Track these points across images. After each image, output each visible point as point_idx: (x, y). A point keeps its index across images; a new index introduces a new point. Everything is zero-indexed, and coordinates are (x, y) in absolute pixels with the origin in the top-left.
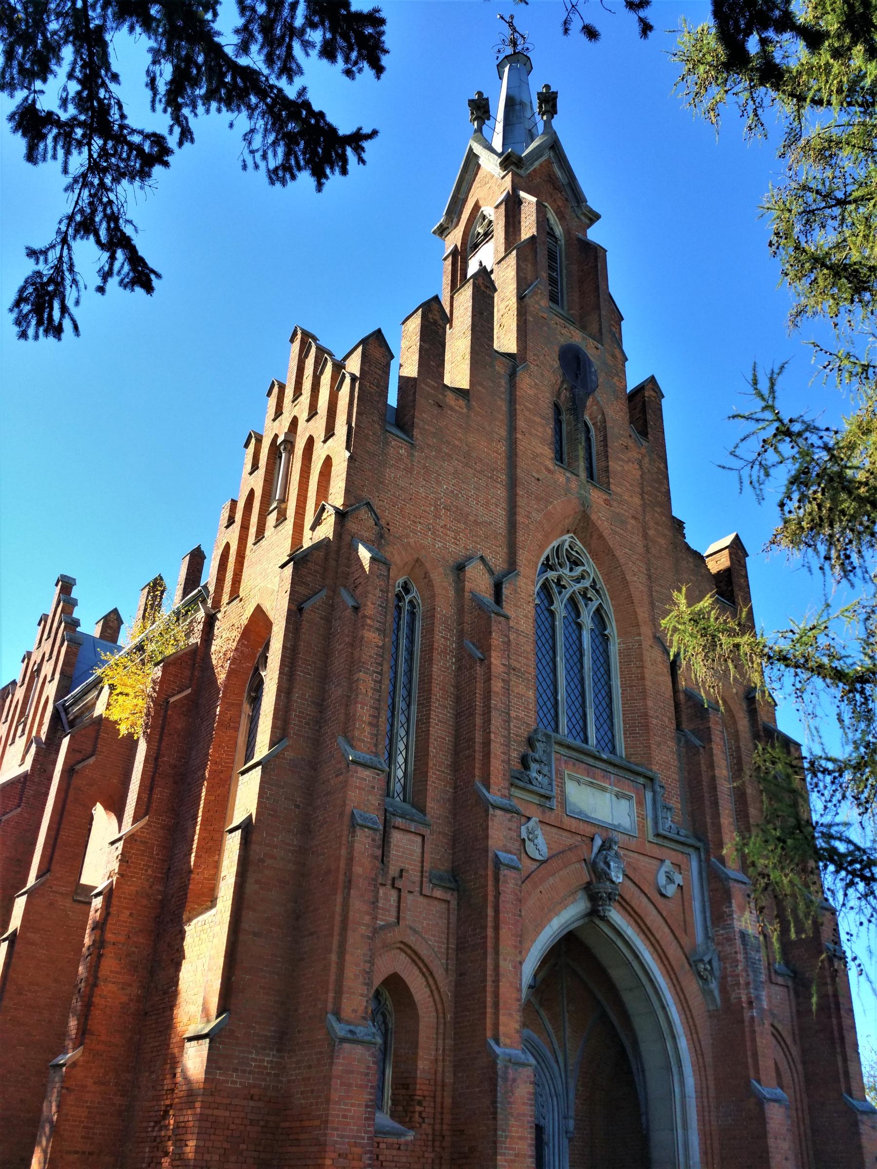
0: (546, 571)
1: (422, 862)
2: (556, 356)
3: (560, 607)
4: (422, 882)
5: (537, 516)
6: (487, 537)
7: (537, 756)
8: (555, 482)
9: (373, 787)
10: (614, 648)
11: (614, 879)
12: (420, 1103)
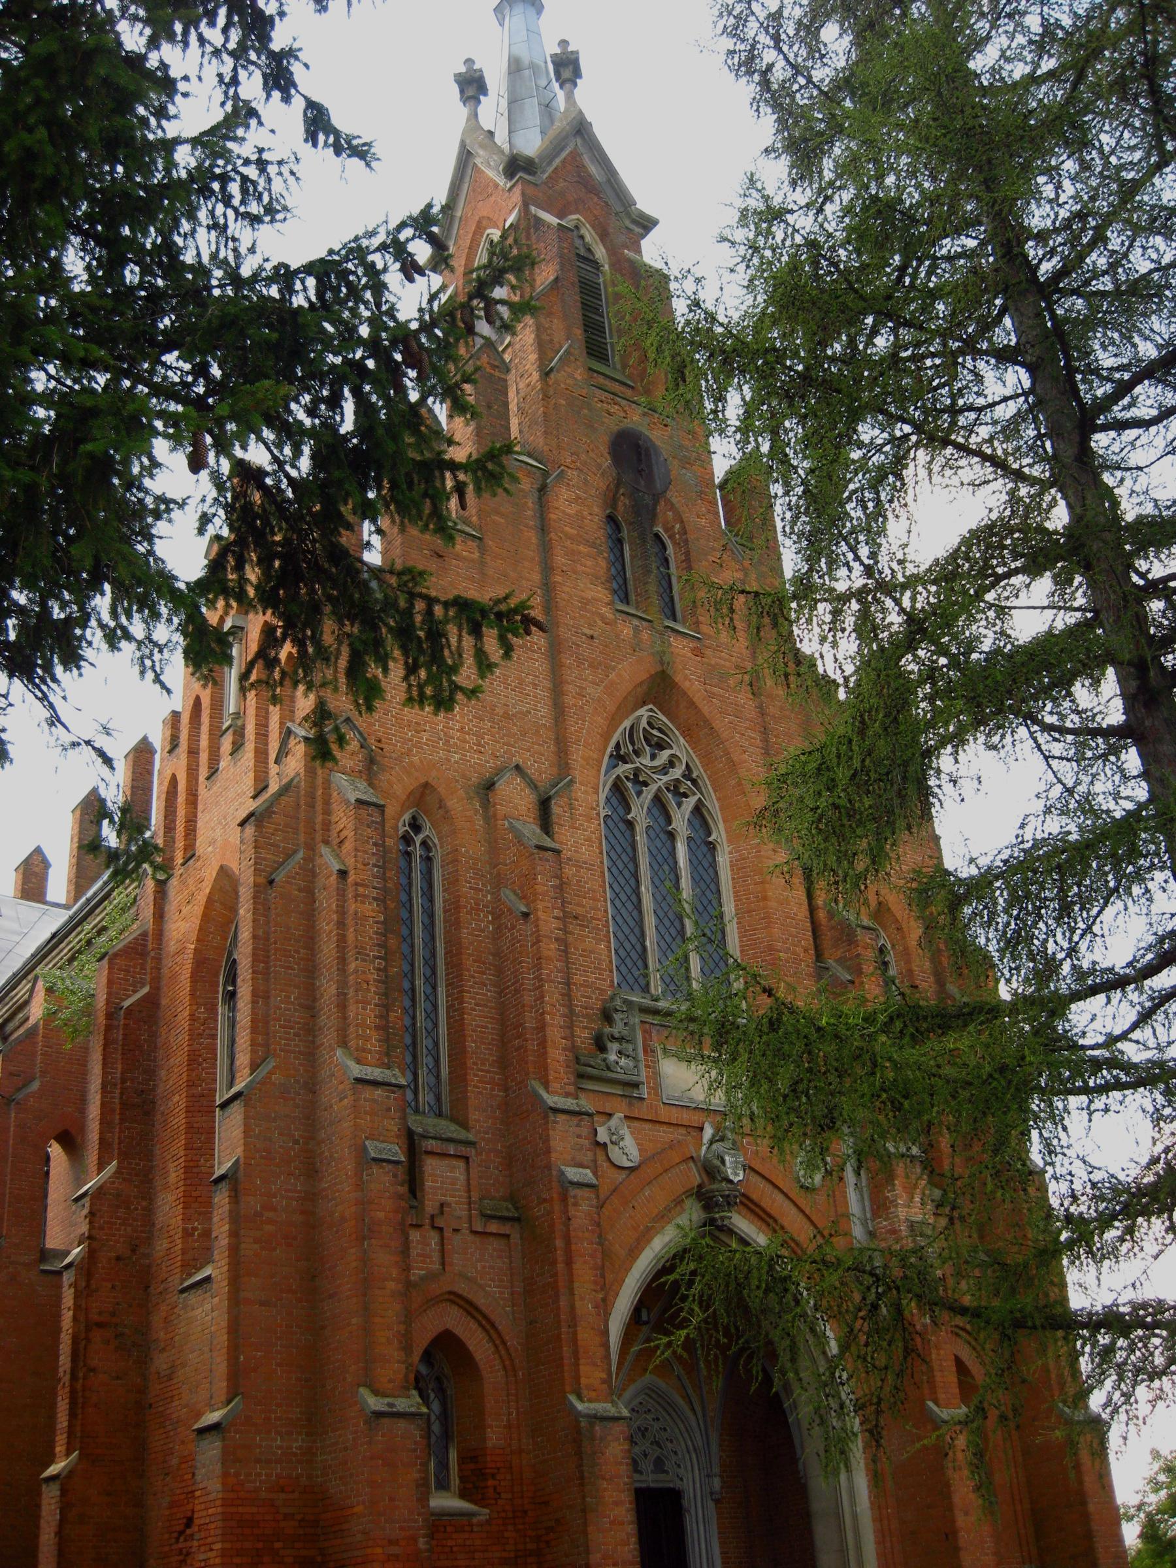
0: (616, 766)
1: (469, 1191)
2: (604, 449)
3: (640, 810)
4: (470, 1216)
5: (594, 691)
6: (524, 734)
7: (615, 1031)
8: (617, 636)
9: (389, 1110)
10: (723, 860)
11: (732, 1177)
12: (493, 1476)
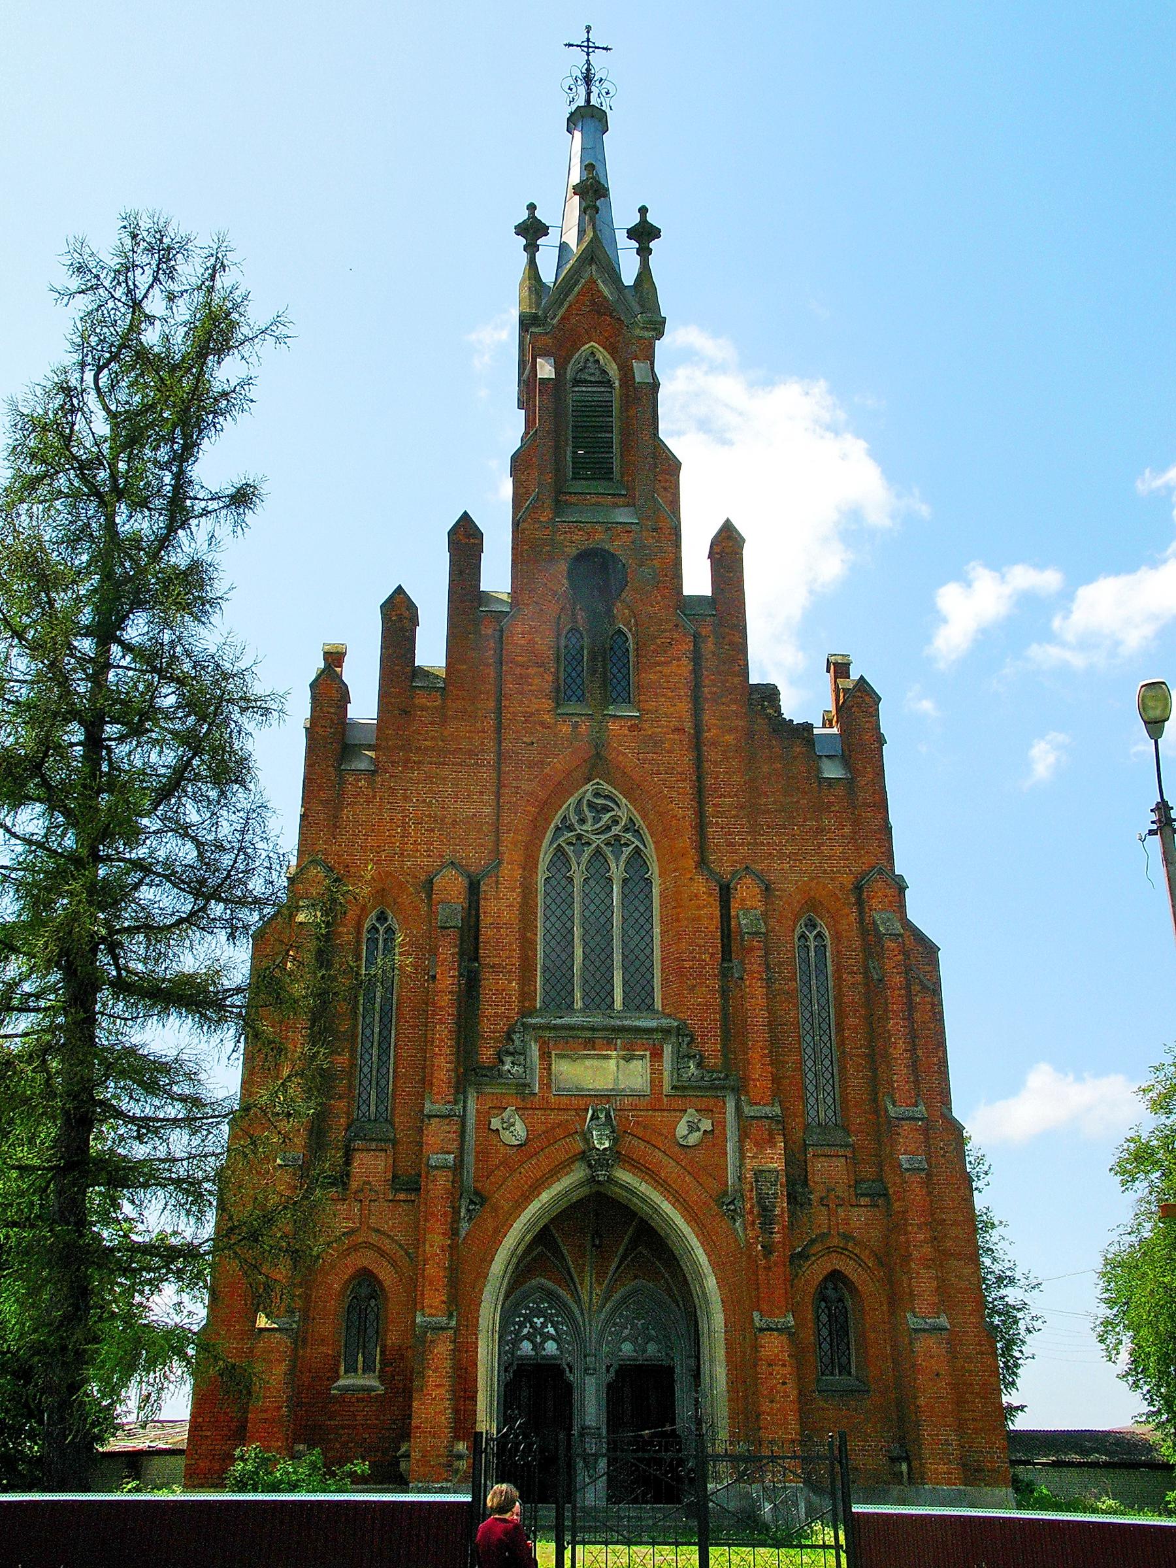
8: (555, 735)
